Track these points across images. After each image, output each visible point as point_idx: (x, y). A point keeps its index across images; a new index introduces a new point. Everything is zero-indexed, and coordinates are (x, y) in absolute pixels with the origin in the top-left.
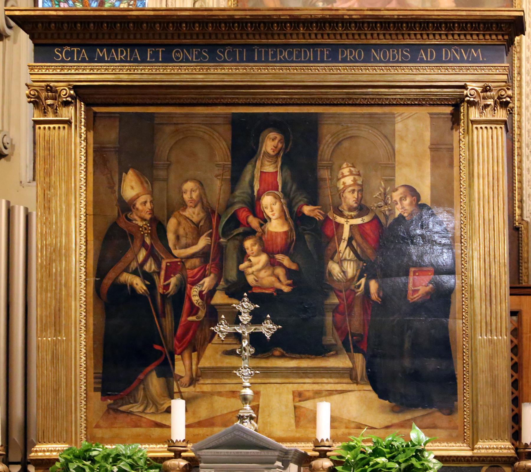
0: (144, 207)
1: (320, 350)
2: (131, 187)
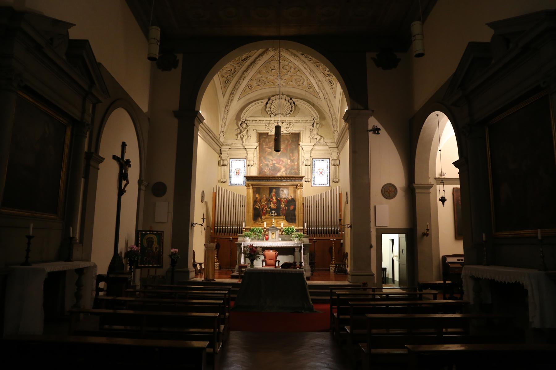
0: (259, 198)
1: (280, 216)
2: (257, 196)
